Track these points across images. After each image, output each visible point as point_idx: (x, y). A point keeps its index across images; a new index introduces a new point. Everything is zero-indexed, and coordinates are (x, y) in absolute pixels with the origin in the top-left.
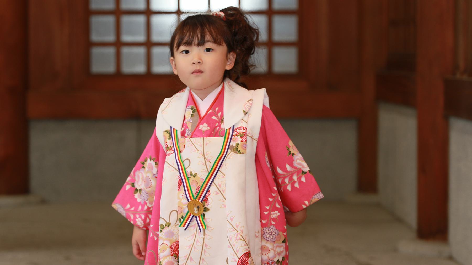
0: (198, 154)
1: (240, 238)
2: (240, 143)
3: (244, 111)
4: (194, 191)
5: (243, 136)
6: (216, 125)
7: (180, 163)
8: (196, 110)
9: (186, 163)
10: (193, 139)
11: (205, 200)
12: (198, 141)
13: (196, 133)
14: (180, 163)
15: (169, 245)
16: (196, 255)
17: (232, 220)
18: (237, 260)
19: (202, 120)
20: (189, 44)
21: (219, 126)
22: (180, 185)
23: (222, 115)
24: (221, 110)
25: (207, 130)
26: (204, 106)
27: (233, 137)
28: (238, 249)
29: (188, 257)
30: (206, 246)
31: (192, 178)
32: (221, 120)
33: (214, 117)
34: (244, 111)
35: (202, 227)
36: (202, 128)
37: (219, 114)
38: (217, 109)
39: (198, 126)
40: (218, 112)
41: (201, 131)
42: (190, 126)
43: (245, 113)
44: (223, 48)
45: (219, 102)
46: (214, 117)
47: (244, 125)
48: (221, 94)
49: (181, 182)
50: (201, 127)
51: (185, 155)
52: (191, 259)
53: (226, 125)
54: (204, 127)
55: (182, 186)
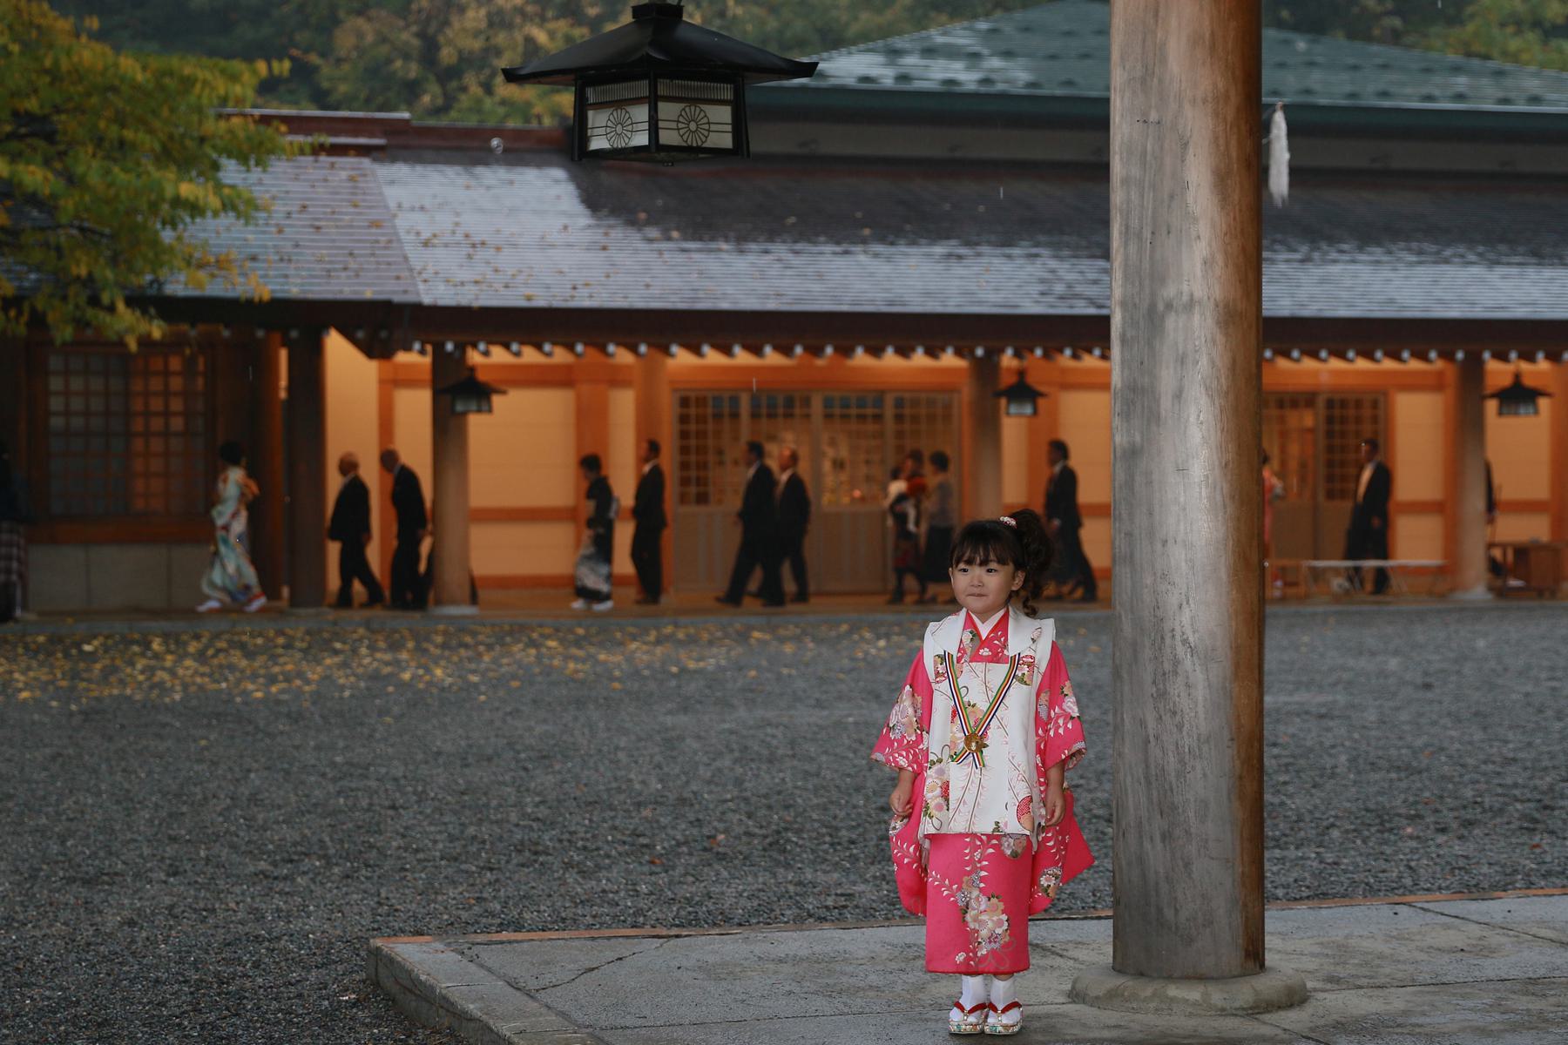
0: (978, 682)
7: (955, 691)
8: (976, 634)
9: (963, 691)
11: (985, 734)
13: (976, 658)
14: (955, 691)
19: (983, 644)
20: (970, 562)
22: (954, 716)
24: (1005, 634)
26: (985, 629)
29: (961, 801)
32: (1005, 646)
35: (981, 764)
44: (1010, 567)
45: (1002, 626)
48: (1005, 617)
49: (955, 713)
51: (961, 682)
53: (1011, 651)
54: (985, 652)
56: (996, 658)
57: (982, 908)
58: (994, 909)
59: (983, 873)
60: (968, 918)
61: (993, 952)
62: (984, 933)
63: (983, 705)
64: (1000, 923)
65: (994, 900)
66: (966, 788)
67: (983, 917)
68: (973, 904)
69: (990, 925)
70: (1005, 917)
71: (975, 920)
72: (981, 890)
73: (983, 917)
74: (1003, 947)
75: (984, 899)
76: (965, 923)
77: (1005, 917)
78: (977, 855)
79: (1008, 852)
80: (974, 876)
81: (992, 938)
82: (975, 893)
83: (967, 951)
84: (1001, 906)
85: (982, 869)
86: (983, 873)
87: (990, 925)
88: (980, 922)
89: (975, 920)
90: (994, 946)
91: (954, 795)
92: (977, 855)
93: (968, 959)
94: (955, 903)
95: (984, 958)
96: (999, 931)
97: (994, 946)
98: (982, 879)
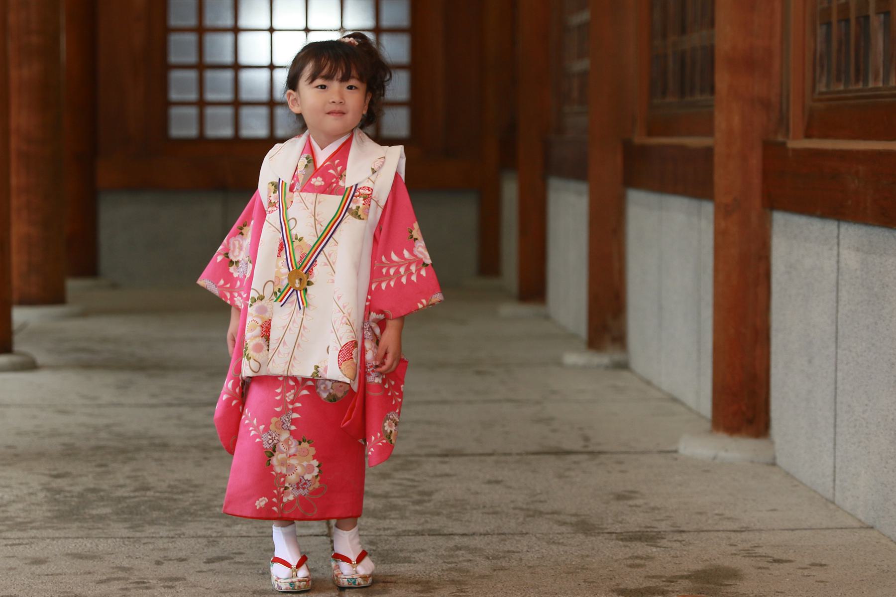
0: (307, 214)
2: (361, 206)
3: (373, 169)
4: (298, 259)
5: (367, 198)
9: (292, 223)
10: (304, 194)
12: (310, 197)
13: (308, 187)
14: (284, 224)
15: (260, 323)
16: (290, 339)
17: (339, 298)
21: (337, 182)
23: (344, 169)
29: (281, 341)
30: (304, 328)
31: (297, 243)
32: (341, 176)
33: (331, 171)
34: (373, 169)
35: (303, 305)
37: (339, 168)
38: (337, 162)
39: (310, 180)
40: (338, 165)
41: (313, 185)
42: (301, 179)
43: (374, 171)
46: (331, 171)
47: (370, 185)
49: (282, 247)
50: (314, 180)
51: (292, 212)
52: (285, 343)
54: (318, 182)
55: (283, 252)
56: (328, 189)
57: (292, 451)
58: (304, 455)
59: (295, 416)
60: (274, 461)
61: (301, 498)
62: (292, 478)
63: (310, 240)
64: (309, 469)
65: (305, 445)
66: (287, 328)
67: (293, 461)
68: (281, 446)
69: (299, 470)
70: (315, 463)
71: (283, 463)
72: (292, 433)
73: (293, 461)
74: (312, 493)
75: (294, 443)
76: (271, 467)
78: (290, 396)
79: (324, 395)
80: (284, 418)
81: (301, 484)
82: (285, 435)
83: (270, 496)
84: (313, 451)
85: (295, 410)
86: (295, 416)
87: (299, 470)
88: (290, 467)
89: (283, 463)
90: (302, 492)
91: (274, 335)
93: (270, 504)
94: (261, 443)
95: (290, 504)
96: (308, 477)
97: (301, 491)
98: (294, 422)
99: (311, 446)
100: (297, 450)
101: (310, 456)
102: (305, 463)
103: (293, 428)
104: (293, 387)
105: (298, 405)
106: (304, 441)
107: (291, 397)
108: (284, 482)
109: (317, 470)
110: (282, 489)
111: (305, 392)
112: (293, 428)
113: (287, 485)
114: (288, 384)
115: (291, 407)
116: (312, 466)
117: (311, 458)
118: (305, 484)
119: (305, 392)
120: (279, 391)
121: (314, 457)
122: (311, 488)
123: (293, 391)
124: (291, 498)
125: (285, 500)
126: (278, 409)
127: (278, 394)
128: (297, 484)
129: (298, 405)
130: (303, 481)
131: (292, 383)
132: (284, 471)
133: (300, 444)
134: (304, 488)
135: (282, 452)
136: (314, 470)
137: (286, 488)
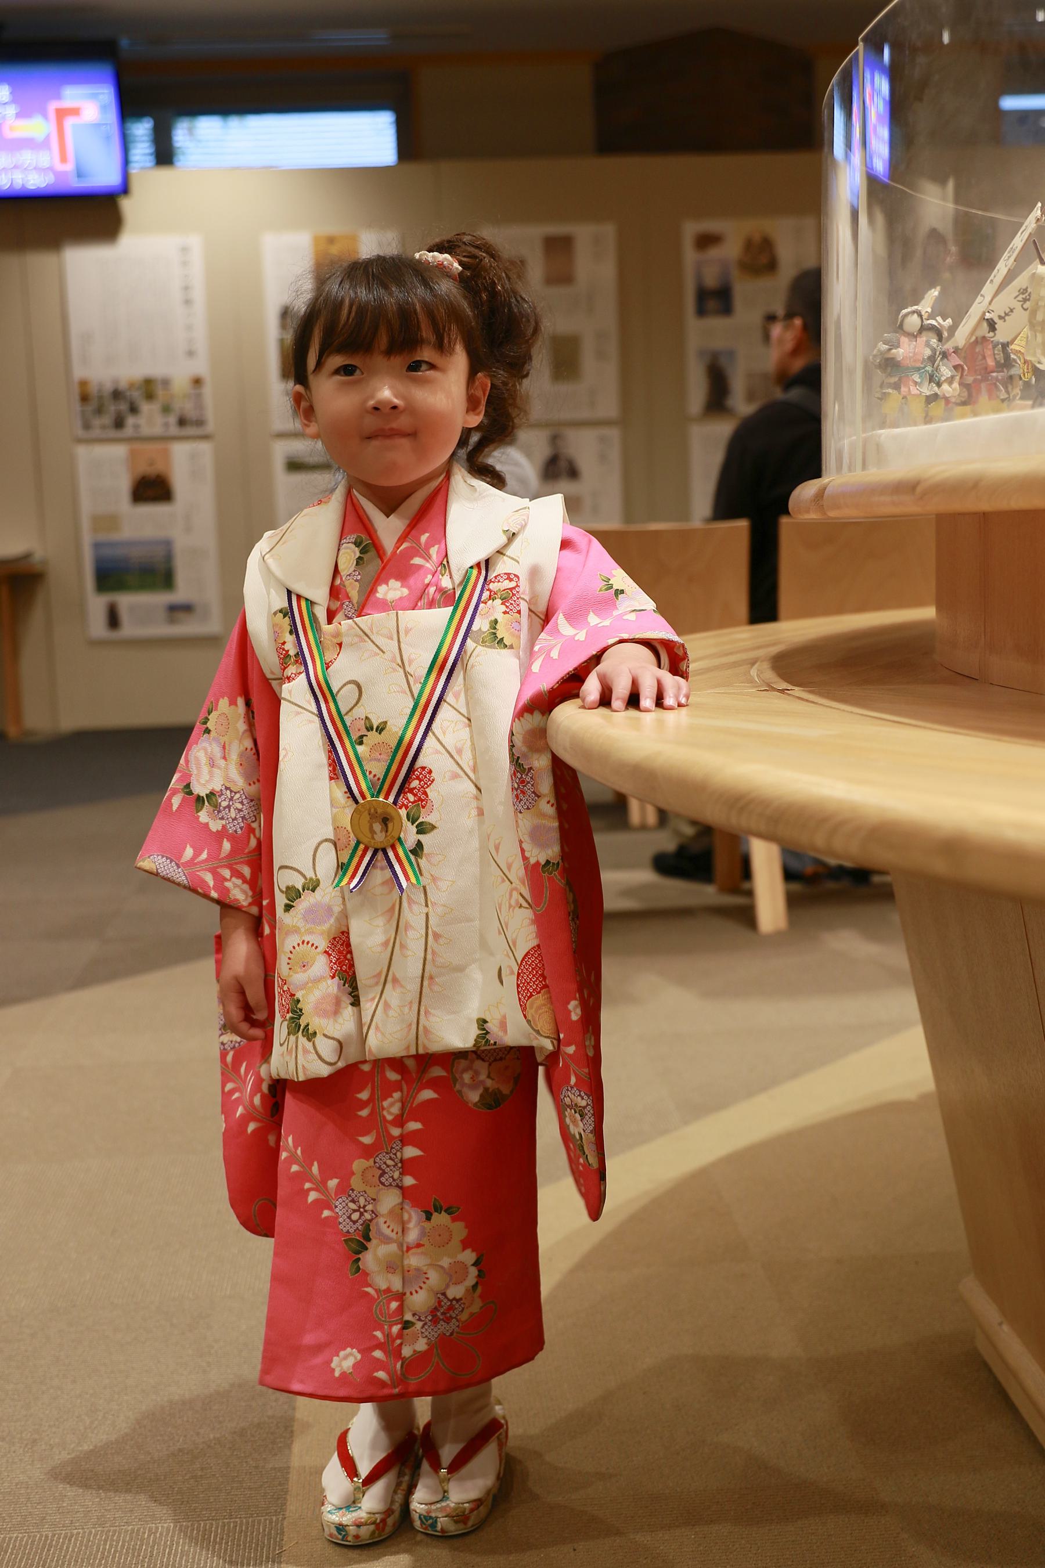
1: (517, 901)
6: (427, 581)
9: (346, 698)
18: (516, 969)
25: (401, 598)
27: (482, 605)
28: (514, 936)
36: (386, 593)
39: (373, 590)
59: (411, 1152)
64: (455, 1274)
65: (441, 1219)
67: (414, 1260)
68: (384, 1226)
69: (434, 1278)
70: (469, 1257)
75: (414, 1217)
77: (469, 1257)
78: (391, 1107)
79: (474, 1097)
80: (383, 1158)
82: (390, 1200)
84: (459, 1230)
85: (405, 1140)
86: (411, 1152)
89: (391, 1267)
92: (391, 1107)
96: (456, 1291)
97: (443, 1327)
98: (407, 1166)
99: (454, 1220)
100: (423, 1233)
101: (456, 1242)
102: (445, 1262)
103: (409, 1181)
104: (397, 1086)
105: (414, 1126)
106: (438, 1210)
107: (396, 1110)
108: (401, 1310)
109: (473, 1272)
110: (395, 1329)
111: (428, 1094)
112: (409, 1181)
113: (408, 1317)
114: (385, 1080)
115: (396, 1132)
116: (465, 1267)
117: (460, 1246)
118: (451, 1308)
119: (428, 1094)
120: (364, 1095)
121: (465, 1244)
122: (464, 1317)
123: (397, 1095)
124: (421, 1345)
125: (407, 1352)
126: (367, 1140)
127: (363, 1105)
128: (434, 1311)
129: (414, 1126)
130: (446, 1304)
131: (393, 1076)
132: (397, 1285)
133: (428, 1218)
134: (448, 1320)
135: (387, 1240)
136: (466, 1274)
137: (407, 1325)
